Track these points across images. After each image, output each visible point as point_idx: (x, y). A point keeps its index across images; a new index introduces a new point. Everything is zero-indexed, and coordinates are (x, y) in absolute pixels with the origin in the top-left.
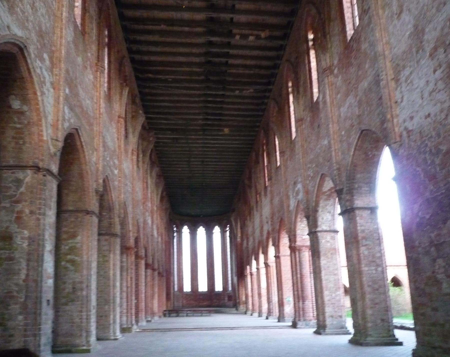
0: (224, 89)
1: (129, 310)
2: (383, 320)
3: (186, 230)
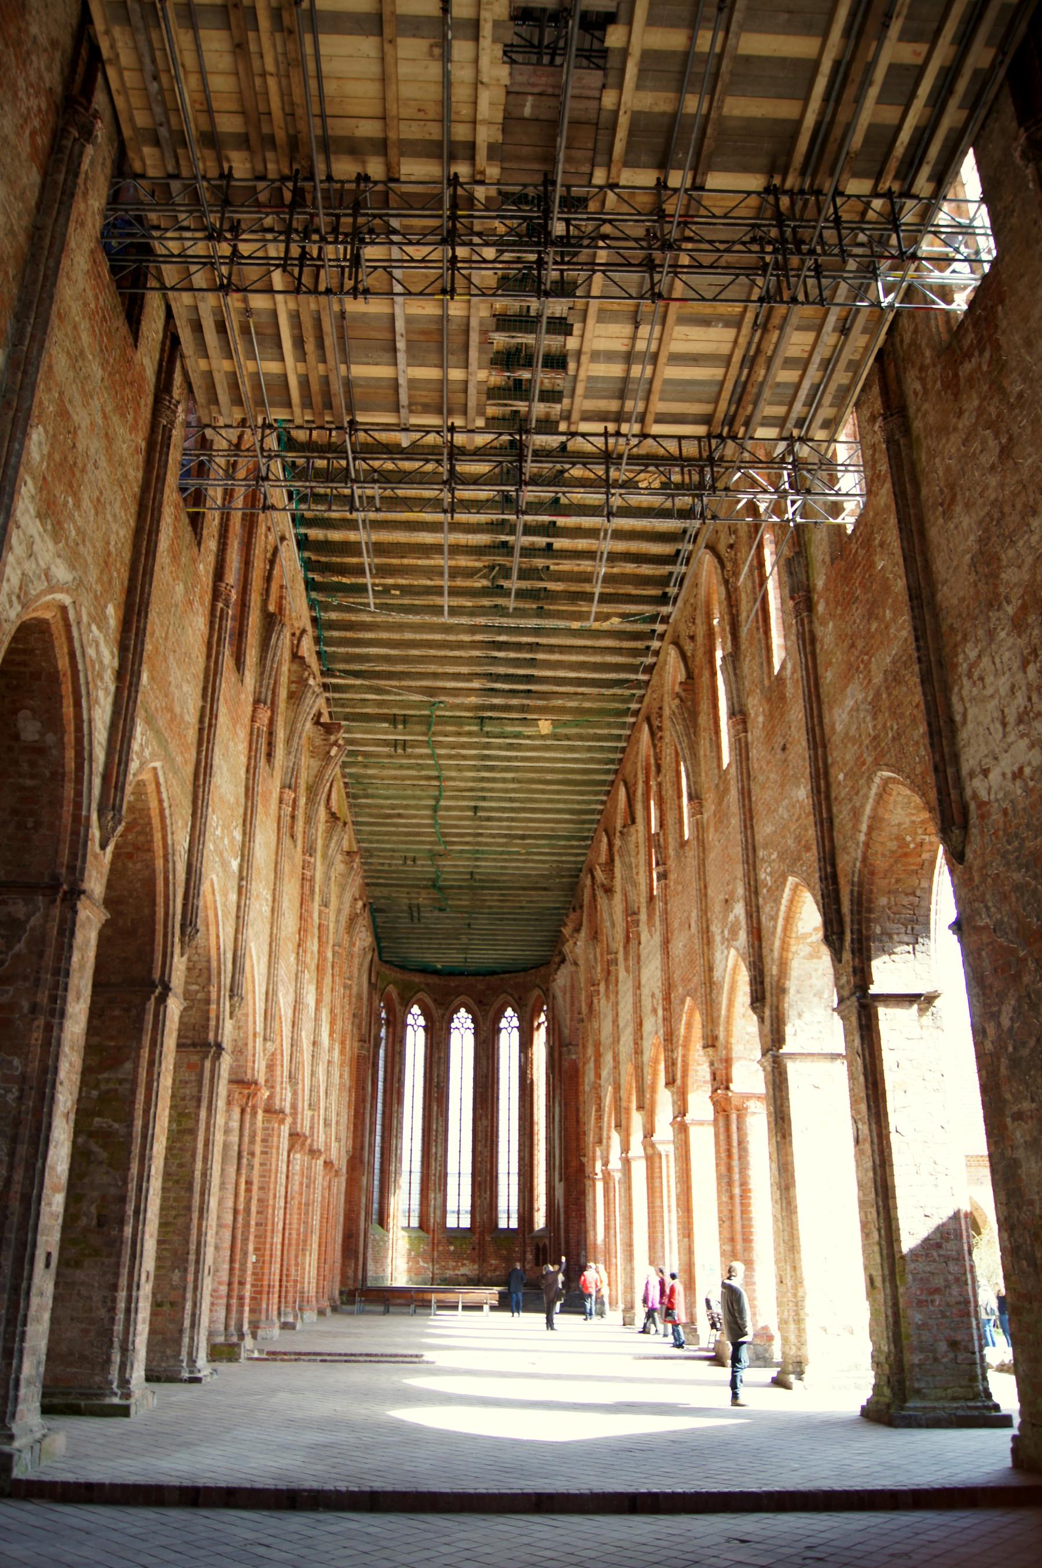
1: (236, 1286)
2: (954, 1345)
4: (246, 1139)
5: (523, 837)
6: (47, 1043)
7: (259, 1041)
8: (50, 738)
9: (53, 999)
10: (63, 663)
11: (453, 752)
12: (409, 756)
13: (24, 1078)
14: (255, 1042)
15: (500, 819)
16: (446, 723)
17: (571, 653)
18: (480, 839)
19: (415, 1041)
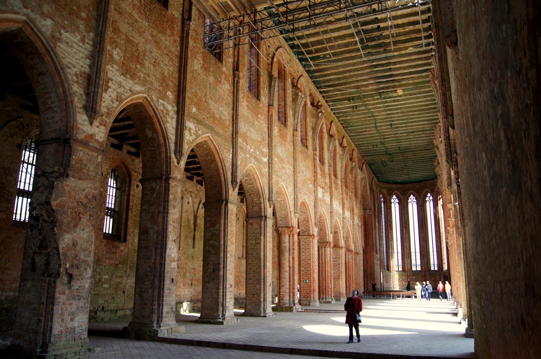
0: (385, 51)
1: (291, 289)
3: (394, 200)
4: (291, 245)
5: (413, 132)
6: (163, 222)
7: (293, 214)
8: (155, 135)
9: (164, 209)
10: (151, 113)
11: (374, 106)
12: (360, 111)
13: (157, 231)
15: (402, 127)
16: (367, 97)
17: (402, 64)
18: (397, 135)
19: (395, 208)
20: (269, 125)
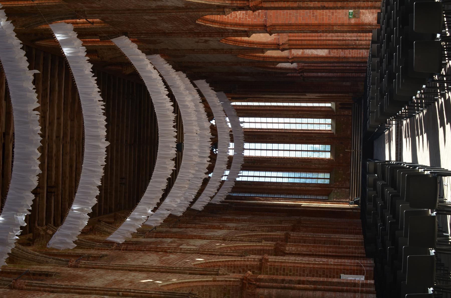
7: (218, 278)
14: (218, 281)
20: (45, 291)
